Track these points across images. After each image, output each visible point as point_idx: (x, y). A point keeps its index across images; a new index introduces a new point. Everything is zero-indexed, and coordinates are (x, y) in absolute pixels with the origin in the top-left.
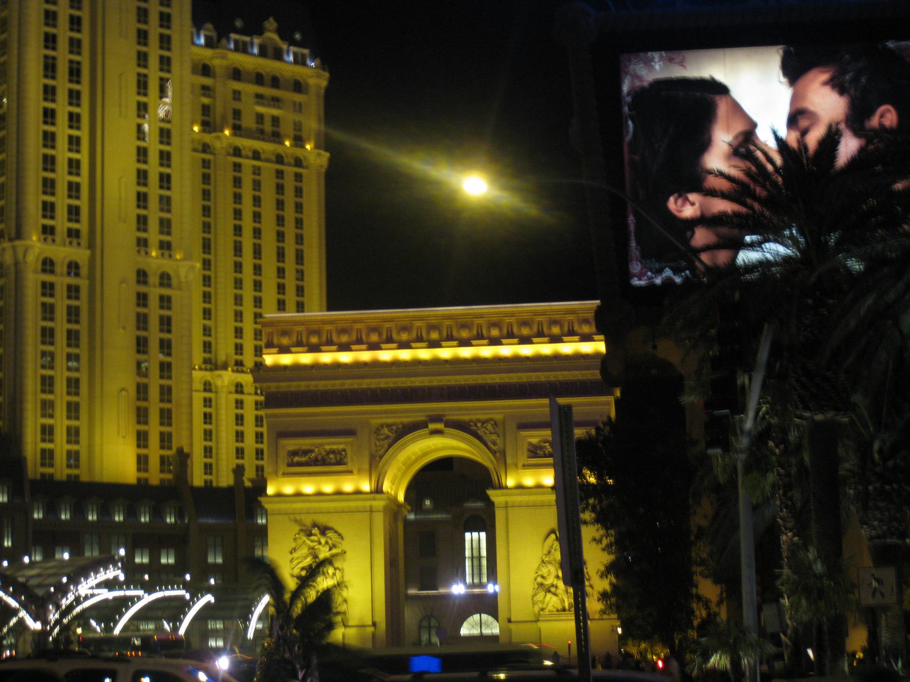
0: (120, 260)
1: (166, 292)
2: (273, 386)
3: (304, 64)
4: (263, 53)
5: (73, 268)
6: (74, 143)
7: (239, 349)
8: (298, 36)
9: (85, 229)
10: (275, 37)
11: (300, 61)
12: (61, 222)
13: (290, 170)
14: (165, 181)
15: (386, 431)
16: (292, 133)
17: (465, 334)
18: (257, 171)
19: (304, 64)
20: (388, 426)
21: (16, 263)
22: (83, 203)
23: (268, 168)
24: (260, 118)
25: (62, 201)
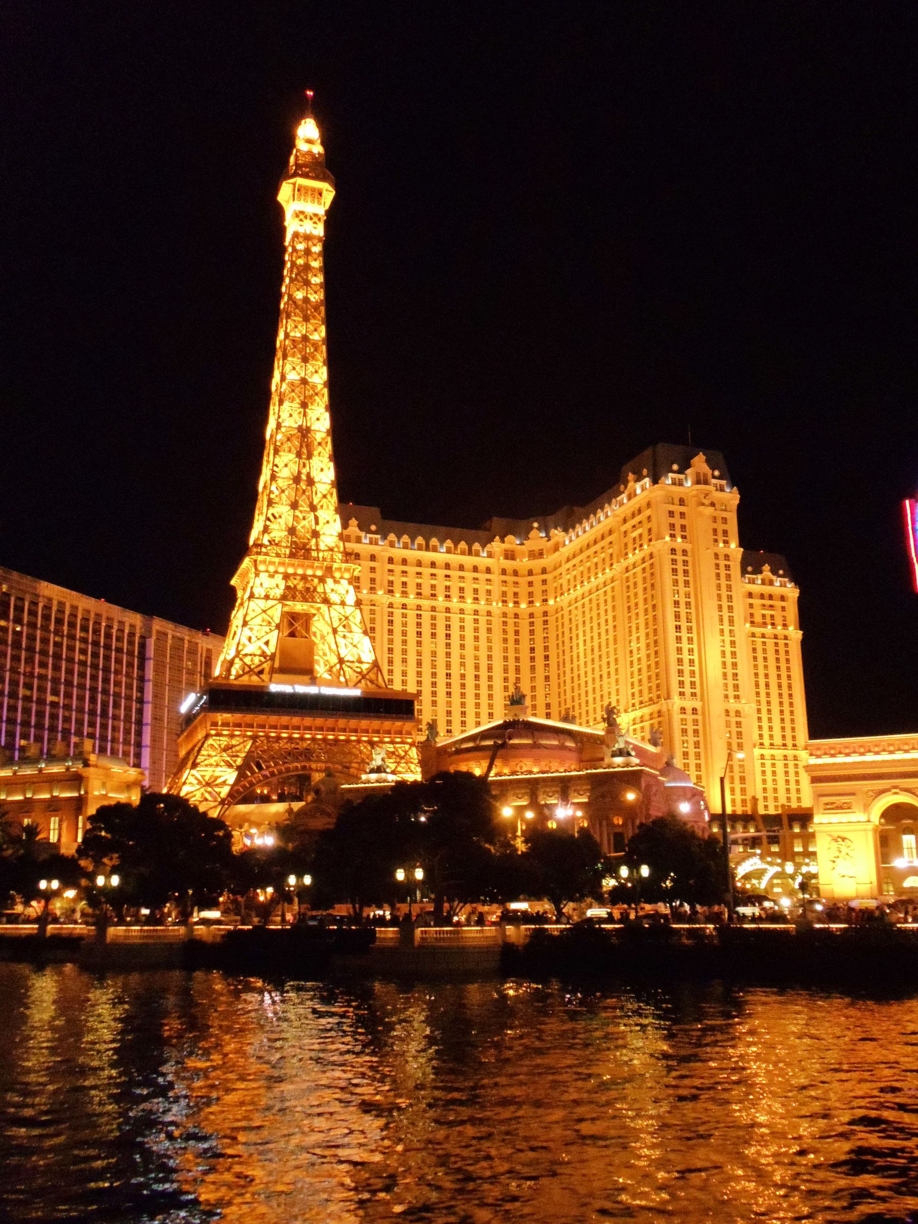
0: (717, 707)
1: (738, 719)
2: (815, 774)
3: (785, 586)
4: (763, 583)
5: (694, 711)
6: (691, 651)
7: (761, 736)
8: (781, 572)
9: (698, 690)
10: (770, 574)
11: (783, 585)
12: (688, 690)
13: (782, 642)
14: (734, 665)
15: (871, 793)
16: (782, 623)
17: (906, 747)
18: (764, 643)
19: (785, 586)
20: (872, 791)
21: (668, 711)
22: (697, 679)
23: (770, 642)
24: (764, 616)
25: (687, 679)
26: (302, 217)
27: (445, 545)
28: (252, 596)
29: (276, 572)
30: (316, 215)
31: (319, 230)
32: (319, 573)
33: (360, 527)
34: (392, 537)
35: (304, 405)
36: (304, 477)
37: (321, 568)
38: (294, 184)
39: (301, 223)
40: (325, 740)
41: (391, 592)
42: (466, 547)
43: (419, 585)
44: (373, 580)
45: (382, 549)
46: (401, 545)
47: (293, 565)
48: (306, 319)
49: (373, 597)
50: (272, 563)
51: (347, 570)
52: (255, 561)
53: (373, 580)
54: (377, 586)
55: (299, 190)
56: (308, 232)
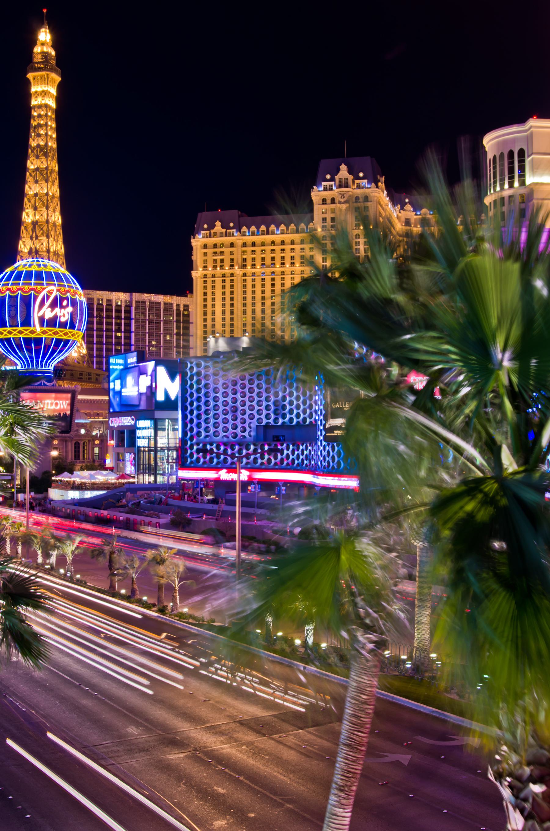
27: (280, 228)
30: (43, 91)
33: (223, 227)
34: (244, 229)
35: (35, 209)
36: (34, 250)
41: (244, 266)
42: (295, 228)
43: (263, 259)
44: (232, 260)
45: (236, 238)
48: (37, 157)
49: (232, 271)
53: (232, 260)
54: (235, 263)
55: (34, 79)
56: (39, 103)
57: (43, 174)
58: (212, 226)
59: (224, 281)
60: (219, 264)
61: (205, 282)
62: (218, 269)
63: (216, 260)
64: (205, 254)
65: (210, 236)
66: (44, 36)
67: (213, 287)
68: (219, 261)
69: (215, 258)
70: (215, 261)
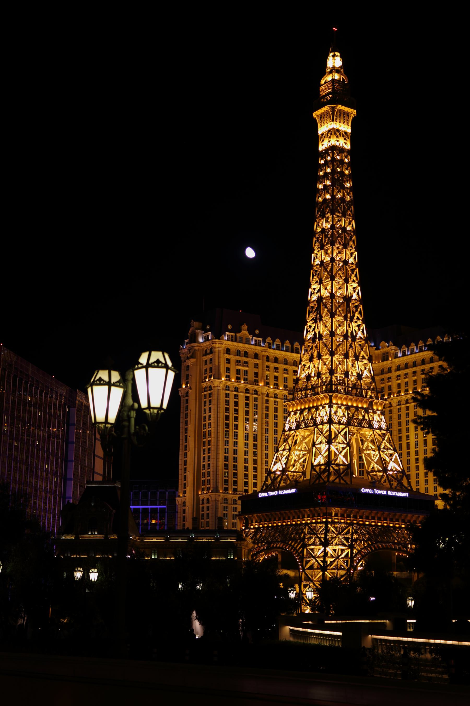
26: (338, 134)
28: (330, 421)
29: (342, 405)
30: (346, 133)
31: (348, 146)
32: (365, 406)
34: (269, 340)
36: (349, 335)
37: (366, 402)
38: (333, 109)
39: (337, 139)
40: (376, 525)
41: (267, 384)
43: (286, 380)
46: (275, 347)
47: (351, 400)
50: (341, 398)
51: (381, 404)
52: (331, 397)
54: (259, 379)
57: (332, 237)
58: (236, 329)
59: (247, 398)
60: (242, 376)
61: (228, 395)
62: (242, 382)
63: (239, 370)
64: (228, 361)
65: (235, 341)
66: (335, 61)
67: (236, 403)
68: (242, 373)
69: (239, 367)
70: (238, 371)
